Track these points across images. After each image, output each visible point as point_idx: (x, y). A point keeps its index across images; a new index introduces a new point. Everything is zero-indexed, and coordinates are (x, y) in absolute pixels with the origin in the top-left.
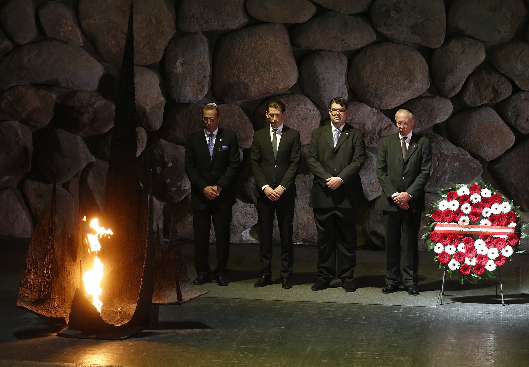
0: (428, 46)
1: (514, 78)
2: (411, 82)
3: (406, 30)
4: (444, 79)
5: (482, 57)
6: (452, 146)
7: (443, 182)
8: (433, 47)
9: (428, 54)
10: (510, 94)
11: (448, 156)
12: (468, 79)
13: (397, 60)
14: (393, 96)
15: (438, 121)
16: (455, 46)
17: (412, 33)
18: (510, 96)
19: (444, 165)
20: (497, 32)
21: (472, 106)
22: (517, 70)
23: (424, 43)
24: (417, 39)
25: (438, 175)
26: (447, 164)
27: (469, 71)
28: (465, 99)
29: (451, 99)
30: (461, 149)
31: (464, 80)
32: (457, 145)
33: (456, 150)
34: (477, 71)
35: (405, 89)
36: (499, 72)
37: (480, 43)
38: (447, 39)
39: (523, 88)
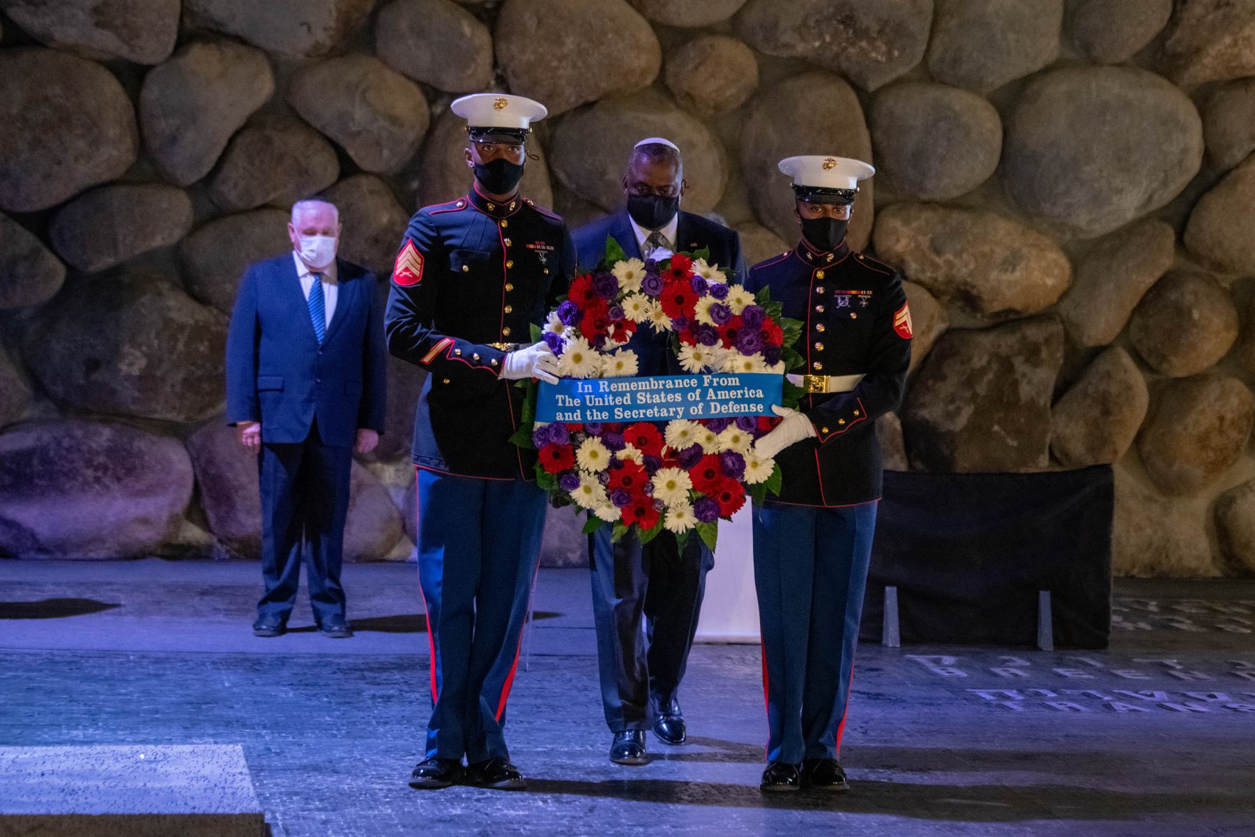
0: (134, 57)
1: (344, 142)
2: (95, 143)
3: (81, 15)
4: (173, 139)
5: (265, 87)
6: (193, 305)
7: (168, 389)
8: (146, 60)
9: (133, 76)
10: (335, 178)
11: (182, 327)
12: (232, 140)
13: (58, 90)
14: (47, 176)
15: (158, 242)
16: (200, 57)
17: (98, 25)
18: (334, 185)
19: (174, 348)
20: (305, 28)
21: (241, 205)
22: (353, 120)
23: (124, 52)
24: (107, 41)
25: (158, 373)
26: (180, 346)
27: (237, 120)
28: (224, 189)
29: (190, 190)
30: (215, 311)
31: (224, 142)
32: (202, 300)
33: (203, 314)
34: (252, 123)
35: (76, 160)
36: (308, 125)
37: (260, 57)
38: (184, 41)
39: (365, 165)
